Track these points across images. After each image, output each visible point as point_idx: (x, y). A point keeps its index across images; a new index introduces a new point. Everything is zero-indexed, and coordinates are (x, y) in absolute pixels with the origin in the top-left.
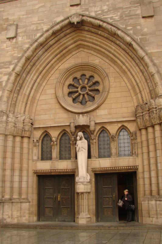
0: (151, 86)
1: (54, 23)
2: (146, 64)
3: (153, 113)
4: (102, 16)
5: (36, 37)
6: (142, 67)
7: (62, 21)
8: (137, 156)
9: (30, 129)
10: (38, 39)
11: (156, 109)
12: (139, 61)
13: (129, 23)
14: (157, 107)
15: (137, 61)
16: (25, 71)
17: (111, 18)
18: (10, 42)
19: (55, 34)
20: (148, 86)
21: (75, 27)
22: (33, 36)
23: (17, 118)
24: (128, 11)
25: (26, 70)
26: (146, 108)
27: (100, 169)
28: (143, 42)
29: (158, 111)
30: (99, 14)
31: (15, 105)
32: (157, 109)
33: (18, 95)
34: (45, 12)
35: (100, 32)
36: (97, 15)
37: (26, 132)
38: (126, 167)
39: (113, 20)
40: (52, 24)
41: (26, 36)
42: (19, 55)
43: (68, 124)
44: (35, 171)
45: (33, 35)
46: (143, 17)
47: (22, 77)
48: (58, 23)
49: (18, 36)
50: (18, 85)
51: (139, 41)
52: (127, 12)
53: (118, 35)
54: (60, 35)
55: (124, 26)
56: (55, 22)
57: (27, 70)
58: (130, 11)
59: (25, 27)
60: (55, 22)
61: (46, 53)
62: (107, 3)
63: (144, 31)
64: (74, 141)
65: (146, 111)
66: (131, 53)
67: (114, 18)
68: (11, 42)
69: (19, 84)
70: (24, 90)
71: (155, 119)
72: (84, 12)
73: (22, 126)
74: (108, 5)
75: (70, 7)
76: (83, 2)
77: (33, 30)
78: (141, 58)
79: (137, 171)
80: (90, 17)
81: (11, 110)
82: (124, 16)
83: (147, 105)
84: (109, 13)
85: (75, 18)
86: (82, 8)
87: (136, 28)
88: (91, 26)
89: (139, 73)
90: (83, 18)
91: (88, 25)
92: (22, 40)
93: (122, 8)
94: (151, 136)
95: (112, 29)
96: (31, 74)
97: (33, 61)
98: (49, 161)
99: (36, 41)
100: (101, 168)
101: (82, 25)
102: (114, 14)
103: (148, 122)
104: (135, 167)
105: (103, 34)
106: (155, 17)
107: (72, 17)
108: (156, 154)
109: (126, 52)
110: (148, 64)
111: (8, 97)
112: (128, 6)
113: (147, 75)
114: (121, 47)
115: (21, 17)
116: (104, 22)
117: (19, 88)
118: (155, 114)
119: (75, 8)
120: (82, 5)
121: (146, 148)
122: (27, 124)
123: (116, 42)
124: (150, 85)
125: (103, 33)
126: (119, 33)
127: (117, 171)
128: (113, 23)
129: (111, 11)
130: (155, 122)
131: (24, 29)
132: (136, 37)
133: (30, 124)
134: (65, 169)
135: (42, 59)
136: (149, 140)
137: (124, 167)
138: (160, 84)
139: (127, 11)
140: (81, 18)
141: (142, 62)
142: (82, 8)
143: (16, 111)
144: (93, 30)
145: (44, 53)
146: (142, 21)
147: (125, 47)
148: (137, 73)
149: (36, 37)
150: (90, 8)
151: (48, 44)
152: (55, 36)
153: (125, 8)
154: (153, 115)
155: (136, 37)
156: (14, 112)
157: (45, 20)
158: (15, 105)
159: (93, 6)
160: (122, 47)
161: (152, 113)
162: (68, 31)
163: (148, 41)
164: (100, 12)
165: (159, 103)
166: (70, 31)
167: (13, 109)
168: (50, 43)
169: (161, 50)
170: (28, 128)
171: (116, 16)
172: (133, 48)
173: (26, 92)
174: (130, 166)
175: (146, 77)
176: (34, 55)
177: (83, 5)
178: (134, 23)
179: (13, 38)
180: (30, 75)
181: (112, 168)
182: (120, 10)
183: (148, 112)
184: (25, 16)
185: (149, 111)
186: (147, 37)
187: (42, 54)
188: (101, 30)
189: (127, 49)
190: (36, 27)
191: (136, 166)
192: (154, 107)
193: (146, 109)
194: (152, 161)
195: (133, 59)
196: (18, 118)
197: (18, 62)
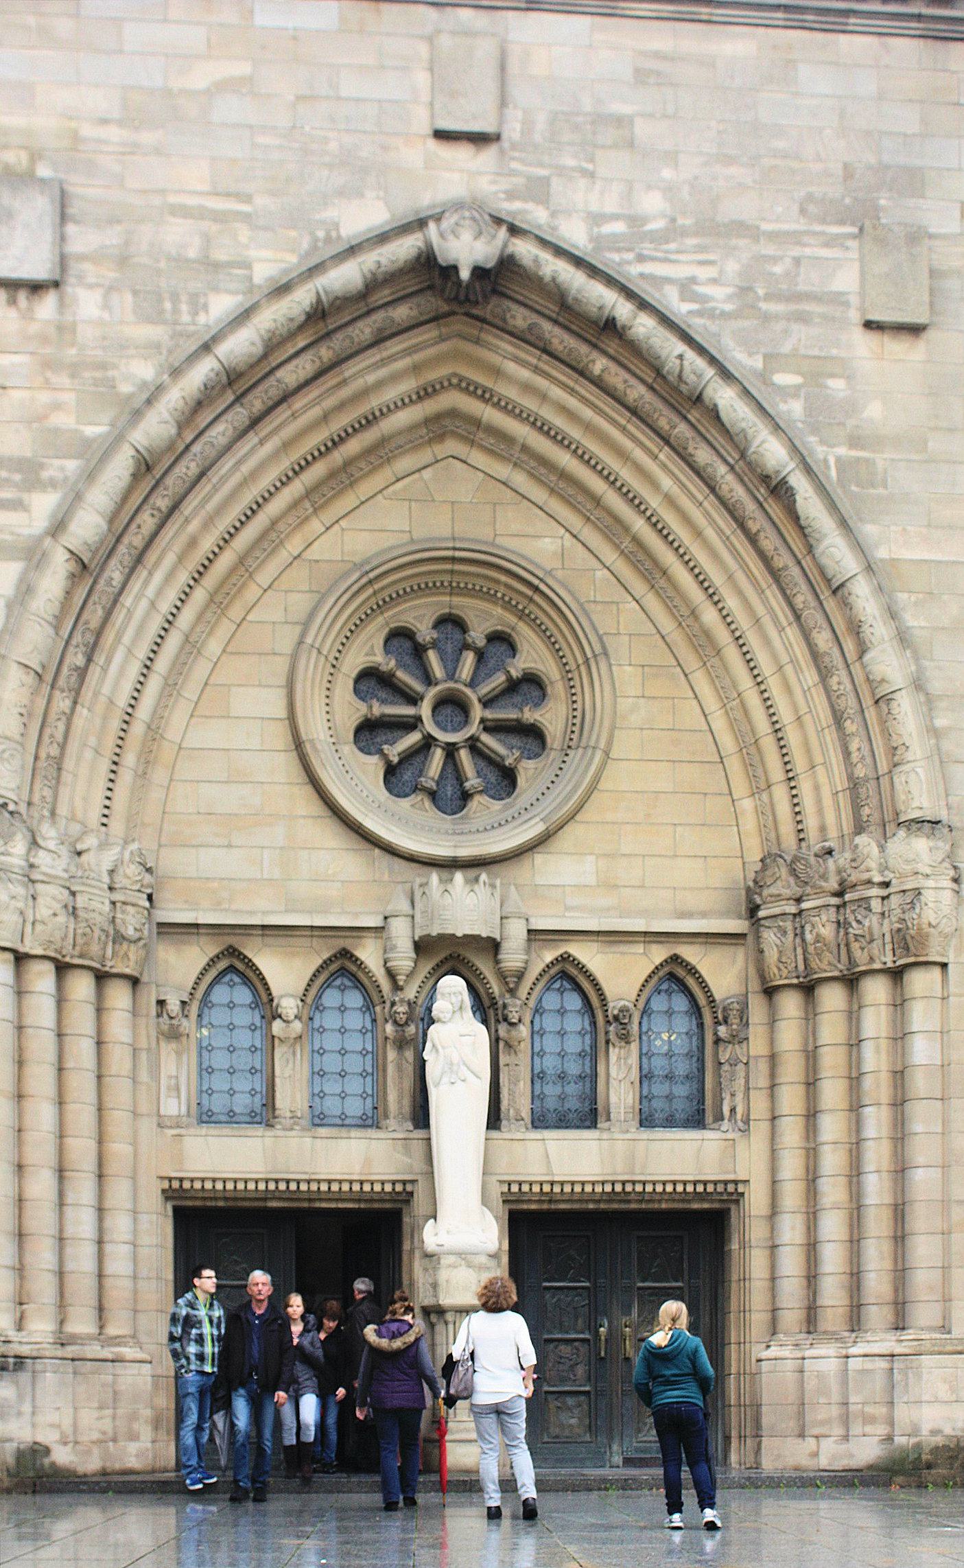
0: (863, 758)
1: (321, 234)
2: (855, 628)
3: (869, 909)
4: (629, 263)
5: (202, 319)
6: (823, 639)
7: (382, 238)
8: (745, 1131)
9: (146, 932)
10: (216, 339)
11: (884, 892)
12: (810, 597)
13: (786, 348)
14: (894, 881)
15: (803, 597)
16: (122, 549)
17: (687, 288)
18: (12, 313)
19: (319, 314)
20: (847, 754)
21: (456, 298)
22: (184, 307)
23: (79, 854)
24: (788, 261)
25: (126, 540)
26: (824, 877)
27: (547, 1188)
28: (854, 488)
29: (895, 901)
30: (614, 243)
31: (58, 764)
32: (891, 890)
33: (75, 703)
34: (261, 140)
35: (599, 364)
36: (596, 240)
37: (125, 945)
38: (685, 1183)
39: (694, 307)
40: (314, 248)
41: (135, 293)
42: (91, 431)
43: (373, 921)
44: (176, 1184)
45: (184, 298)
46: (869, 325)
47: (102, 582)
48: (353, 250)
49: (72, 280)
50: (77, 638)
51: (833, 473)
52: (778, 269)
53: (714, 414)
54: (350, 329)
55: (758, 363)
56: (328, 233)
57: (135, 539)
58: (797, 261)
59: (119, 222)
60: (334, 234)
61: (252, 439)
62: (667, 173)
63: (865, 415)
64: (406, 1023)
65: (821, 892)
66: (769, 542)
67: (700, 289)
68: (28, 316)
69: (80, 628)
70: (105, 670)
71: (872, 941)
72: (517, 205)
73: (107, 907)
74: (669, 190)
75: (432, 144)
76: (518, 126)
77: (180, 261)
78: (828, 581)
79: (733, 1207)
80: (559, 252)
81: (36, 798)
82: (761, 292)
83: (830, 862)
84: (672, 246)
85: (466, 236)
86: (512, 173)
87: (827, 387)
88: (552, 308)
89: (798, 670)
90: (510, 250)
91: (535, 298)
92: (106, 316)
93: (753, 233)
94: (831, 1030)
95: (686, 363)
96: (150, 574)
97: (169, 481)
98: (260, 1130)
99: (206, 348)
100: (552, 1183)
101: (495, 292)
102: (702, 263)
103: (828, 957)
104: (731, 1188)
105: (617, 378)
106: (930, 334)
107: (445, 224)
108: (857, 1125)
109: (742, 525)
110: (865, 628)
111: (23, 711)
112: (785, 227)
113: (849, 687)
114: (713, 490)
115: (87, 130)
116: (643, 305)
117: (80, 656)
118: (875, 919)
119: (461, 154)
120: (505, 144)
121: (800, 1090)
122: (134, 901)
123: (691, 450)
124: (859, 749)
125: (625, 375)
126: (724, 397)
127: (629, 1201)
128: (699, 327)
129: (684, 233)
130: (872, 960)
131: (112, 237)
132: (820, 451)
133: (145, 896)
134: (351, 1182)
135: (223, 480)
136: (823, 1050)
137: (674, 1183)
138: (919, 755)
139: (775, 260)
140: (505, 245)
141: (830, 604)
142: (512, 173)
143: (63, 810)
144: (555, 341)
145: (242, 434)
146: (863, 344)
147: (740, 493)
148: (789, 669)
149: (202, 319)
150: (556, 185)
151: (272, 380)
152: (321, 328)
153: (773, 236)
154: (867, 923)
155: (819, 451)
156: (53, 813)
157: (261, 201)
158: (59, 769)
159: (573, 169)
160: (724, 490)
161: (864, 912)
162: (402, 313)
163: (885, 487)
164: (619, 227)
165: (907, 862)
166: (414, 313)
167: (47, 793)
168: (280, 374)
169: (939, 557)
170: (133, 921)
171: (714, 281)
172: (795, 517)
173: (117, 684)
174: (705, 1183)
175: (842, 703)
176: (181, 447)
177: (514, 147)
178: (816, 352)
179: (36, 288)
180: (145, 573)
181: (608, 1188)
182: (742, 242)
183: (835, 901)
184: (114, 133)
185: (840, 894)
186: (881, 459)
187: (228, 448)
188: (611, 351)
189: (750, 507)
190: (197, 241)
191: (736, 1182)
192: (877, 879)
193: (823, 884)
194: (832, 1161)
195: (775, 574)
196: (84, 857)
197: (90, 476)
